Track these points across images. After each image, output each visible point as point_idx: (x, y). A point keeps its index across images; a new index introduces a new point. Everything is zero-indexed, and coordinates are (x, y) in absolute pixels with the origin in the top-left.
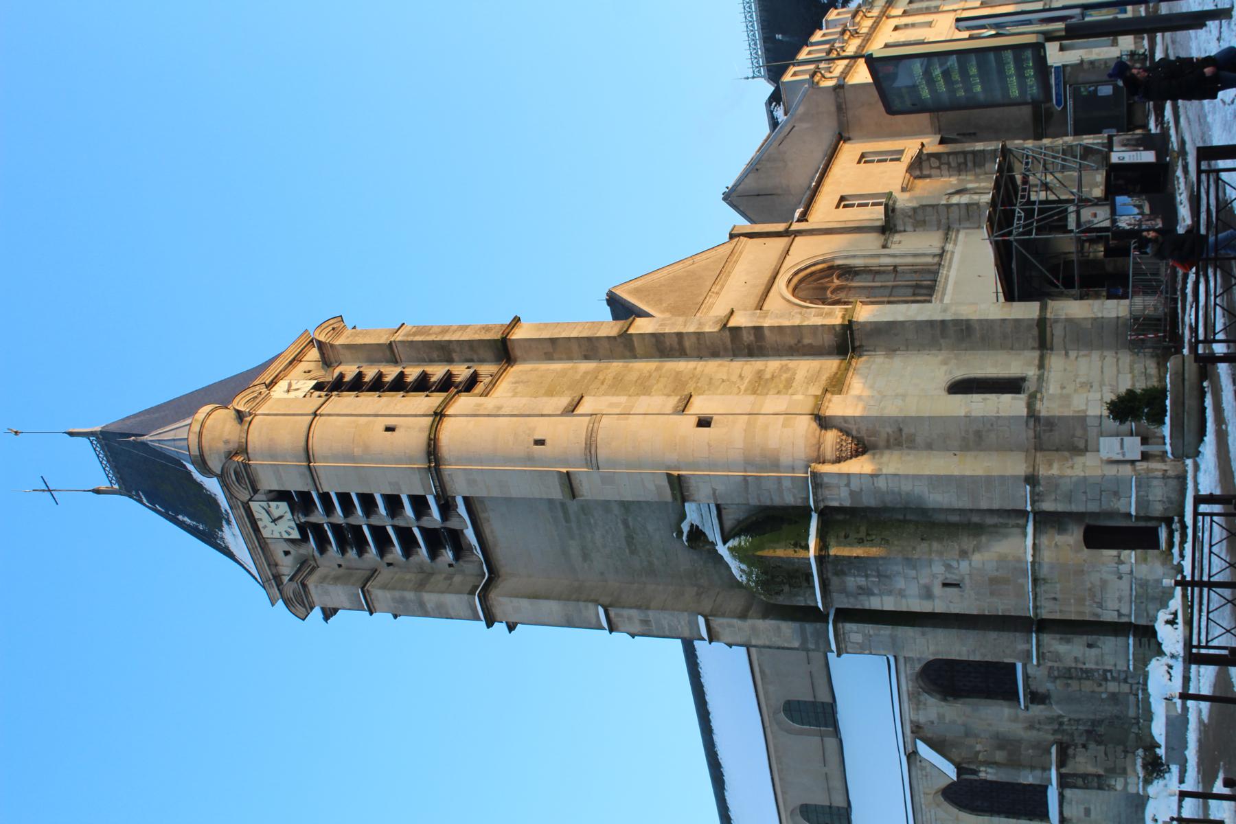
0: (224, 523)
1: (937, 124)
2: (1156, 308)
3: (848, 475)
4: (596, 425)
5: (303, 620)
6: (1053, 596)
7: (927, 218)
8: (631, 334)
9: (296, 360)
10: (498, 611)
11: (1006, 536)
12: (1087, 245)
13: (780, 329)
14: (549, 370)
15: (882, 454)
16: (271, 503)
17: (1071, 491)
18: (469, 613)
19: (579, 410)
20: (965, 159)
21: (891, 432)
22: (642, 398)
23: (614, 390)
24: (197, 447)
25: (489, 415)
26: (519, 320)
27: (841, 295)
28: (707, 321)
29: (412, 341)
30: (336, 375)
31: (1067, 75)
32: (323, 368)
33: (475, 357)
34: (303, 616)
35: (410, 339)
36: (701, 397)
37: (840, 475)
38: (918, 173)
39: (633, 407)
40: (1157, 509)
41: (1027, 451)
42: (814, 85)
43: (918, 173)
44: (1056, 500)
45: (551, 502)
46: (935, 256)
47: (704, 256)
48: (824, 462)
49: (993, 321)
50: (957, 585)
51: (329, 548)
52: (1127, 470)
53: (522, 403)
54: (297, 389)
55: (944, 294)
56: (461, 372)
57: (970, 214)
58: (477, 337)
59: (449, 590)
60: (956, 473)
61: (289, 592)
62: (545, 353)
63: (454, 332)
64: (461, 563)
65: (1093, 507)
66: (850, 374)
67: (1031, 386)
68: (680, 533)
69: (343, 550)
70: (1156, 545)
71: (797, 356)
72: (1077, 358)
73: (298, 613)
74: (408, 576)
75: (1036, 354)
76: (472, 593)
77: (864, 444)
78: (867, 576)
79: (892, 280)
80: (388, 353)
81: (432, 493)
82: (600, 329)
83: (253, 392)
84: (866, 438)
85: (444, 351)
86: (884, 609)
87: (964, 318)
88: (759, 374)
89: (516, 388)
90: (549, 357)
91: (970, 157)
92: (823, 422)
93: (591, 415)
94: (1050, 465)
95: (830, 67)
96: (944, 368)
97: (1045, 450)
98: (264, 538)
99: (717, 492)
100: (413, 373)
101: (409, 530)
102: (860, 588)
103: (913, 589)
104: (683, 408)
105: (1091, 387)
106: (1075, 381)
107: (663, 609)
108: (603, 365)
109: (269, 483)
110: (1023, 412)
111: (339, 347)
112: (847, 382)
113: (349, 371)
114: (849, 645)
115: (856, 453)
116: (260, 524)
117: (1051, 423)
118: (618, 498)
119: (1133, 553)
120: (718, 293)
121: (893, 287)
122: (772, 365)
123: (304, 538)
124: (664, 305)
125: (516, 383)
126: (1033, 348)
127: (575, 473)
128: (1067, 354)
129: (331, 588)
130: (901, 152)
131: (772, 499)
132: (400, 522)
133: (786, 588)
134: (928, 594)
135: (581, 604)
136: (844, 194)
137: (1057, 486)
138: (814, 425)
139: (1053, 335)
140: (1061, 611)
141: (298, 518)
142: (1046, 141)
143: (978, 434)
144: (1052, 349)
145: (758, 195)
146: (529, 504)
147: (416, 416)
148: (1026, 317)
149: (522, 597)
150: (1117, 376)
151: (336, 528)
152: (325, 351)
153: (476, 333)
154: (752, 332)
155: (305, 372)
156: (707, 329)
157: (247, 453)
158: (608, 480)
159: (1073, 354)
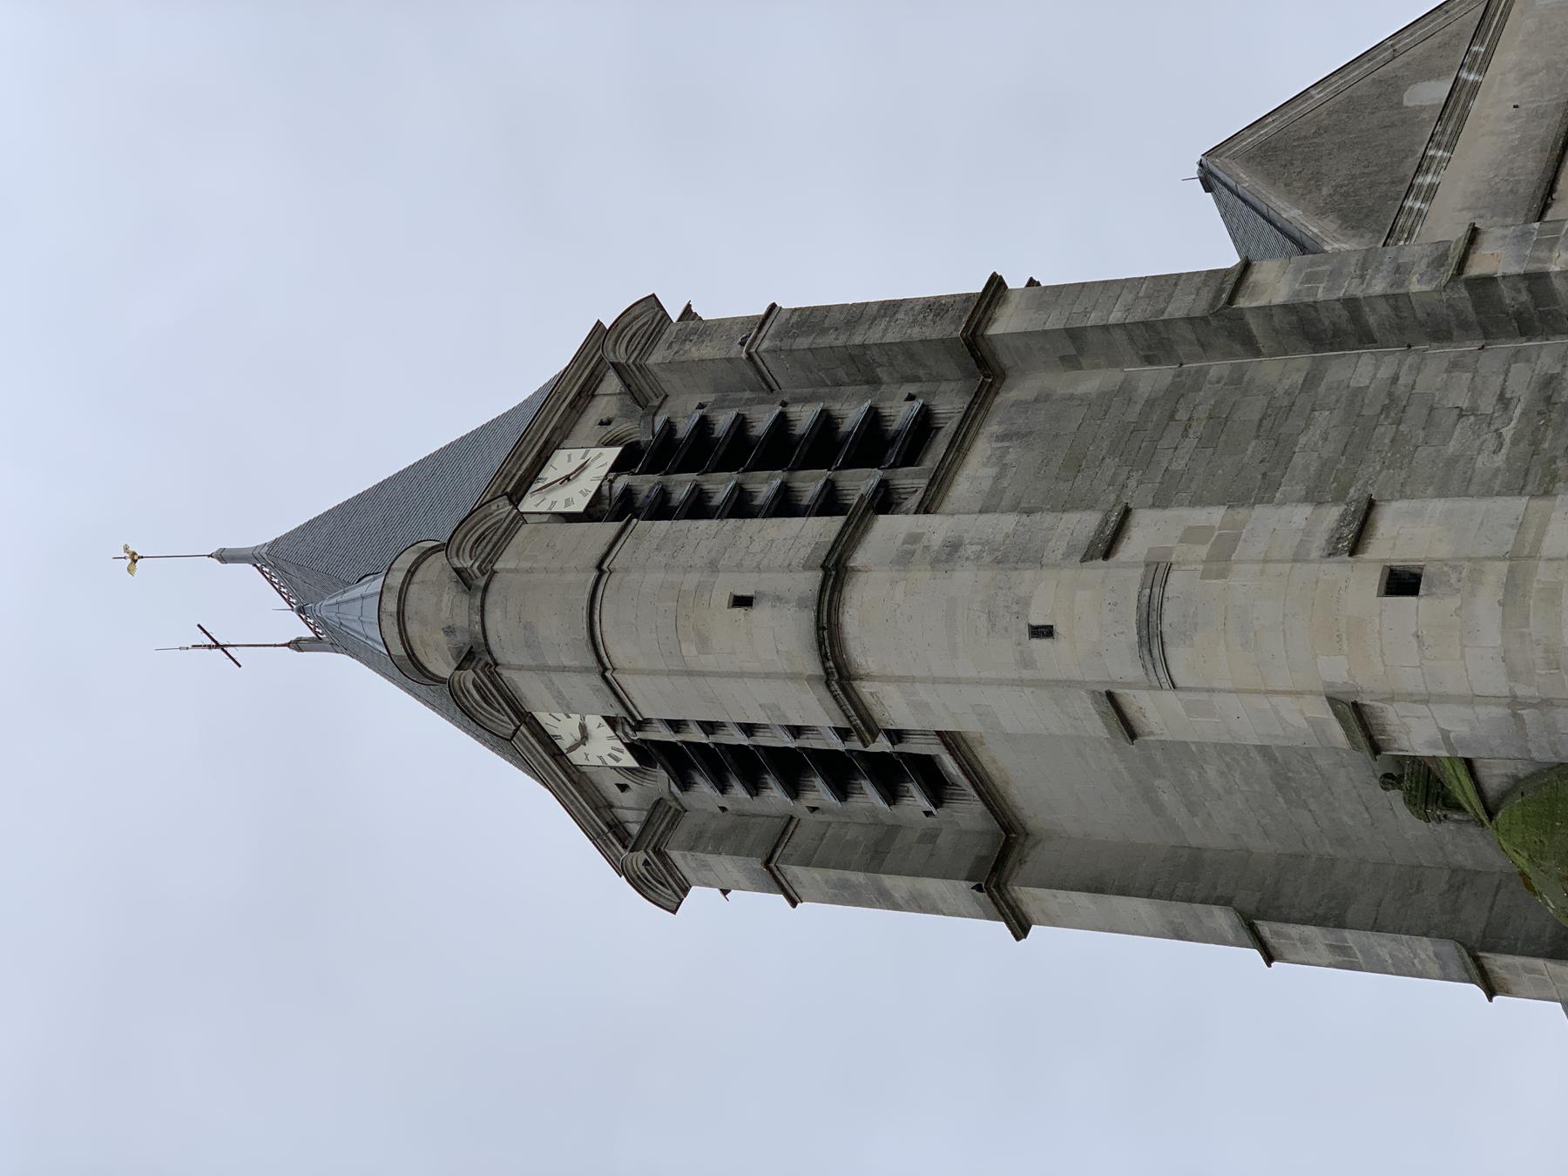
4: (1156, 590)
5: (674, 912)
8: (1241, 309)
22: (1260, 510)
33: (921, 372)
58: (916, 333)
62: (1062, 358)
63: (875, 319)
82: (1171, 296)
89: (1006, 451)
90: (1071, 362)
98: (575, 766)
99: (1452, 735)
107: (1377, 927)
111: (656, 370)
124: (1325, 191)
129: (711, 859)
141: (626, 734)
149: (1072, 890)
152: (629, 381)
154: (1522, 285)
155: (602, 423)
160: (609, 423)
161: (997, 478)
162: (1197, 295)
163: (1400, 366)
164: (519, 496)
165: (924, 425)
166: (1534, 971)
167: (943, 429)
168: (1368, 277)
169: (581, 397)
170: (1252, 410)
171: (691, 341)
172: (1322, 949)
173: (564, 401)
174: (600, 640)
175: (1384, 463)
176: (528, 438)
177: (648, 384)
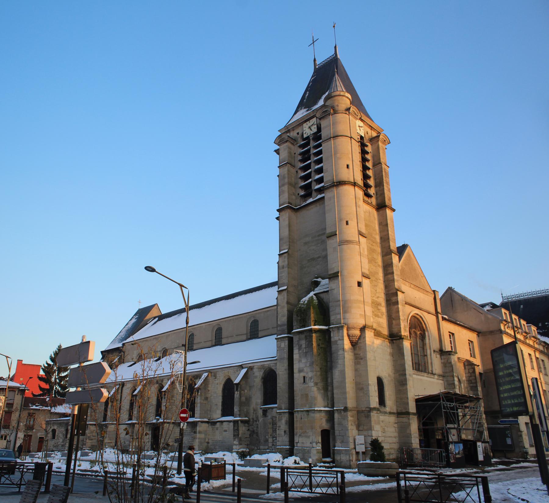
0: (307, 109)
1: (488, 372)
2: (417, 459)
3: (343, 340)
4: (356, 243)
5: (274, 143)
6: (303, 418)
7: (447, 368)
8: (391, 254)
9: (372, 128)
10: (283, 213)
11: (324, 400)
12: (441, 432)
13: (398, 312)
14: (375, 224)
15: (352, 352)
16: (316, 125)
17: (342, 424)
18: (282, 203)
19: (360, 237)
20: (474, 383)
21: (361, 355)
24: (336, 95)
25: (356, 203)
26: (394, 211)
27: (413, 335)
28: (399, 283)
29: (382, 171)
30: (367, 144)
31: (514, 425)
32: (369, 138)
33: (377, 196)
35: (383, 170)
36: (369, 283)
37: (343, 336)
38: (466, 364)
39: (364, 257)
40: (337, 457)
41: (357, 408)
42: (501, 321)
43: (466, 364)
44: (339, 419)
45: (325, 229)
46: (432, 371)
47: (425, 281)
48: (347, 330)
49: (407, 394)
50: (304, 382)
51: (301, 149)
52: (352, 446)
53: (362, 215)
54: (360, 130)
55: (417, 375)
56: (372, 191)
57: (451, 385)
58: (386, 196)
59: (289, 194)
60: (347, 380)
61: (284, 136)
63: (388, 187)
64: (300, 198)
65: (337, 433)
66: (382, 339)
67: (382, 409)
68: (317, 278)
69: (301, 154)
70: (323, 457)
71: (388, 318)
72: (395, 427)
73: (276, 140)
74: (293, 179)
75: (395, 411)
76: (289, 203)
77: (355, 345)
78: (306, 348)
79: (421, 354)
80: (377, 163)
81: (325, 185)
84: (358, 346)
85: (380, 184)
86: (294, 355)
87: (408, 383)
88: (379, 304)
89: (367, 212)
90: (380, 224)
91: (475, 385)
92: (363, 329)
93: (359, 242)
94: (352, 416)
95: (509, 328)
96: (387, 375)
97: (357, 414)
100: (370, 173)
101: (310, 178)
102: (301, 345)
103: (302, 365)
104: (364, 276)
105: (383, 433)
106: (385, 426)
107: (289, 273)
108: (379, 245)
109: (324, 123)
110: (372, 406)
112: (379, 338)
113: (369, 149)
114: (280, 342)
115: (352, 342)
116: (308, 122)
117: (368, 417)
118: (328, 253)
119: (320, 448)
120: (410, 287)
121: (418, 355)
122: (384, 309)
123: (304, 140)
124: (404, 266)
125: (369, 212)
126: (397, 410)
127: (337, 237)
128: (396, 423)
129: (286, 152)
130: (474, 357)
131: (332, 311)
132: (313, 174)
133: (299, 318)
134: (300, 371)
135: (288, 243)
136: (455, 335)
137: (344, 419)
138: (361, 326)
139: (403, 417)
140: (297, 421)
142: (484, 416)
143: (362, 389)
144: (397, 417)
145: (452, 301)
146: (324, 221)
147: (354, 176)
148: (410, 407)
149: (289, 221)
150: (388, 443)
151: (309, 150)
153: (388, 195)
154: (396, 301)
156: (396, 283)
157: (334, 114)
158: (335, 249)
159: (396, 425)
160: (367, 133)
166: (284, 299)
172: (283, 264)
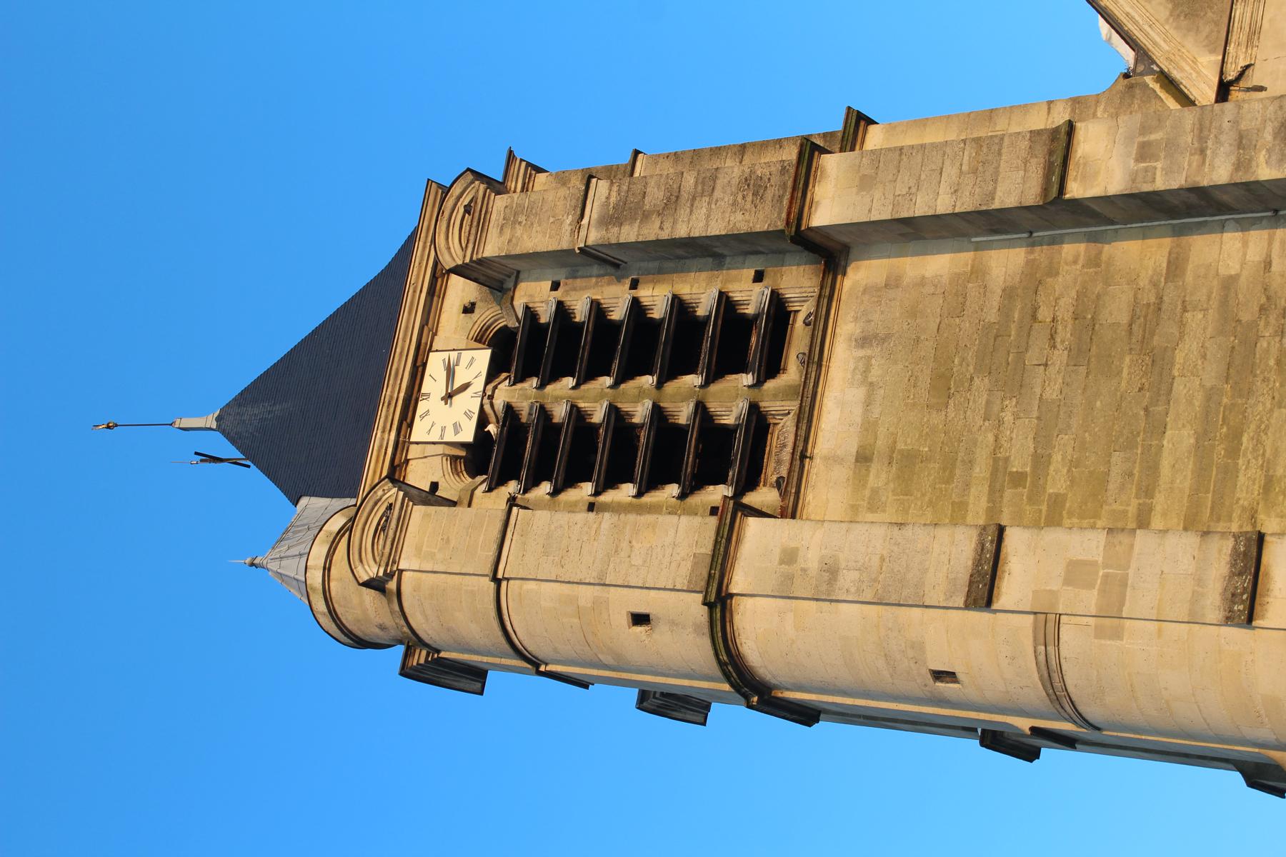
4: (1051, 649)
23: (1083, 370)
30: (520, 313)
34: (703, 721)
63: (694, 198)
83: (376, 504)
108: (1041, 254)
152: (475, 275)
161: (868, 403)
162: (1025, 171)
163: (1270, 243)
164: (409, 420)
165: (779, 311)
167: (801, 312)
168: (1209, 152)
169: (437, 279)
170: (1117, 310)
171: (520, 223)
173: (421, 291)
174: (520, 647)
175: (1273, 398)
176: (398, 350)
177: (494, 271)
